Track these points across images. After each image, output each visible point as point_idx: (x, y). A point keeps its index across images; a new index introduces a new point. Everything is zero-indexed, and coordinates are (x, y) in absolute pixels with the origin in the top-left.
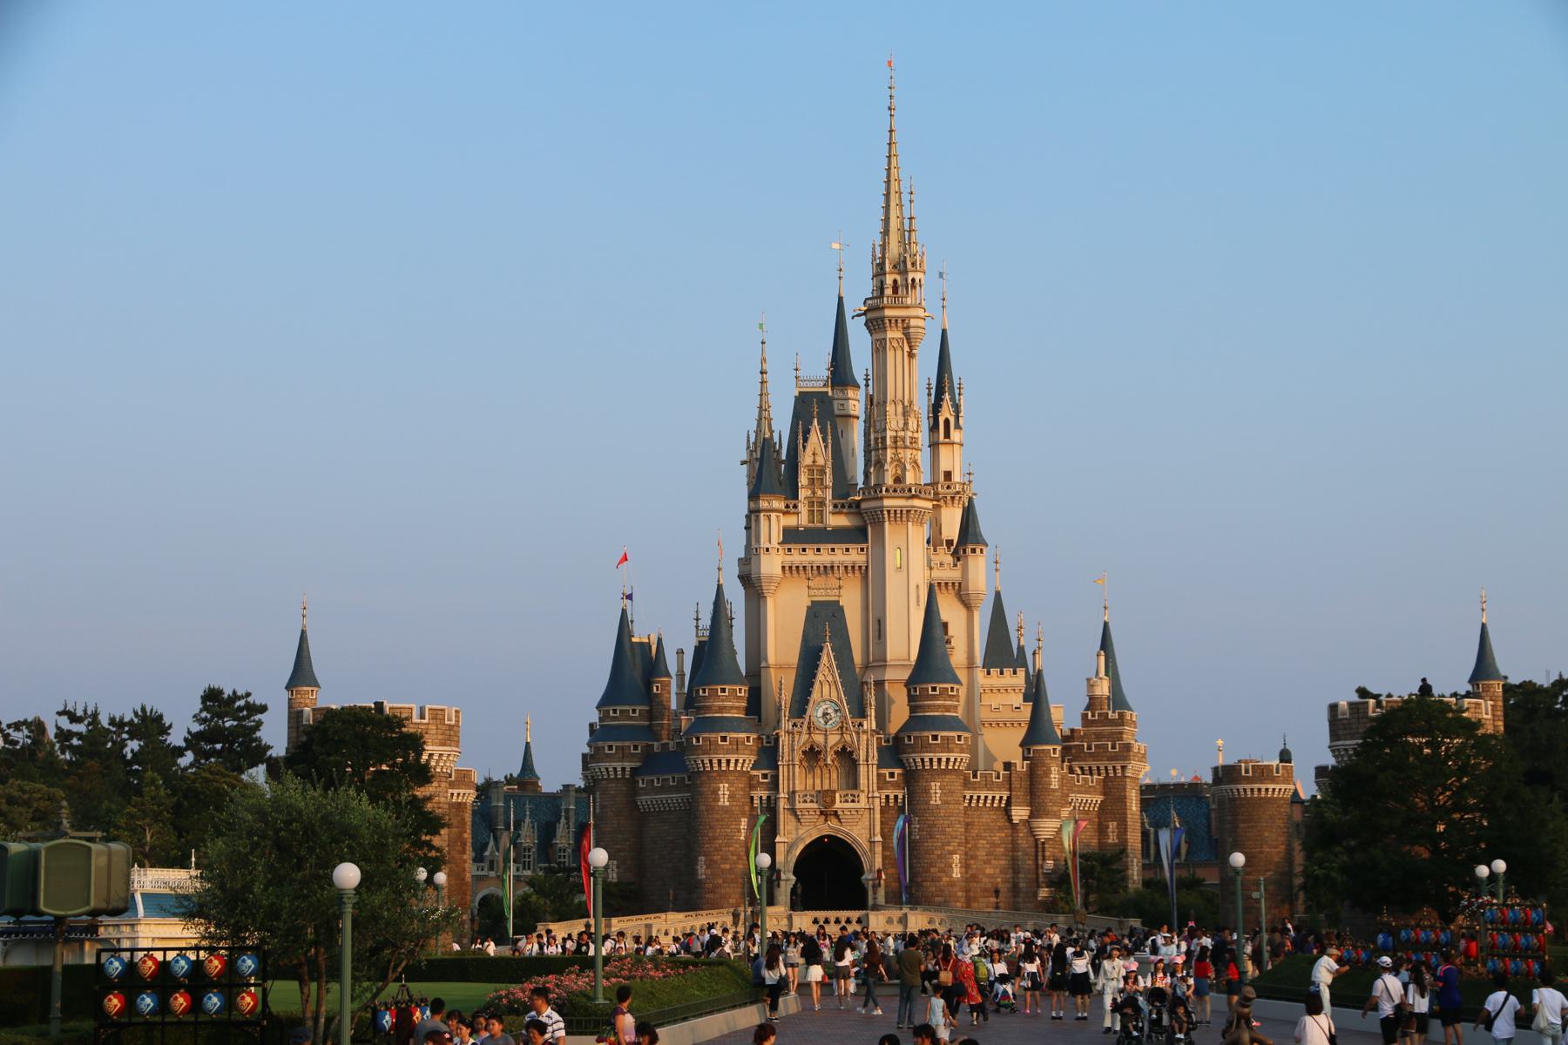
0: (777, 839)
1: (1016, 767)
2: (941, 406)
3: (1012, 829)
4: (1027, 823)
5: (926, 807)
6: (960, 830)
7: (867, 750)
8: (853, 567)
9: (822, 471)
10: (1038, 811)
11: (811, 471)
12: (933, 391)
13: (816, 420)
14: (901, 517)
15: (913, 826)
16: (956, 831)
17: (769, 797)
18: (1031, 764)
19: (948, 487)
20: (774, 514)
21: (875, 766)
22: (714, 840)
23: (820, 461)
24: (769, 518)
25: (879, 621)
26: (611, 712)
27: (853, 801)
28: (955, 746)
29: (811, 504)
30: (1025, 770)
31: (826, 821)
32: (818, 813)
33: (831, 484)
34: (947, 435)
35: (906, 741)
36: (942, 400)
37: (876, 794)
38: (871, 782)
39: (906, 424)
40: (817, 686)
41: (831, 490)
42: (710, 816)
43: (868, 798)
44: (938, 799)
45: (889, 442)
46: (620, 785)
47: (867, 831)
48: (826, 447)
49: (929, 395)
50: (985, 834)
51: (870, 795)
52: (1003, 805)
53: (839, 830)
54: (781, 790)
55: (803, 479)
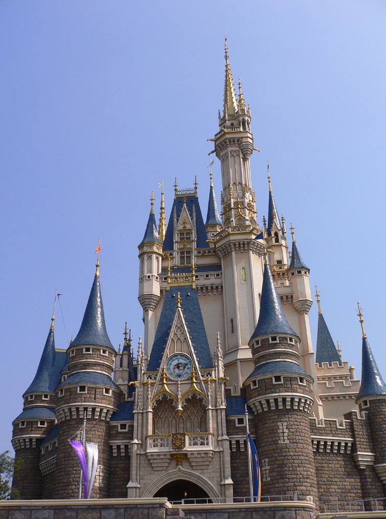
0: (130, 484)
1: (356, 415)
2: (272, 226)
3: (360, 475)
4: (373, 469)
5: (274, 447)
6: (311, 470)
7: (216, 402)
8: (212, 288)
9: (189, 232)
10: (383, 456)
11: (182, 234)
12: (267, 223)
13: (185, 205)
14: (244, 247)
15: (264, 468)
16: (307, 471)
17: (126, 447)
18: (368, 414)
19: (280, 268)
20: (154, 255)
21: (224, 413)
22: (69, 485)
23: (188, 227)
24: (150, 258)
25: (232, 320)
26: (29, 397)
27: (202, 444)
28: (298, 386)
29: (182, 253)
30: (364, 419)
31: (177, 465)
32: (168, 457)
33: (196, 239)
34: (277, 241)
35: (252, 387)
36: (272, 223)
37: (225, 437)
38: (220, 425)
39: (244, 194)
40: (169, 342)
41: (195, 242)
42: (67, 462)
43: (218, 441)
44: (286, 438)
45: (232, 206)
46: (28, 454)
47: (218, 475)
48: (192, 219)
49: (265, 224)
50: (336, 480)
51: (220, 438)
52: (349, 452)
53: (191, 474)
54: (135, 436)
55: (176, 238)
